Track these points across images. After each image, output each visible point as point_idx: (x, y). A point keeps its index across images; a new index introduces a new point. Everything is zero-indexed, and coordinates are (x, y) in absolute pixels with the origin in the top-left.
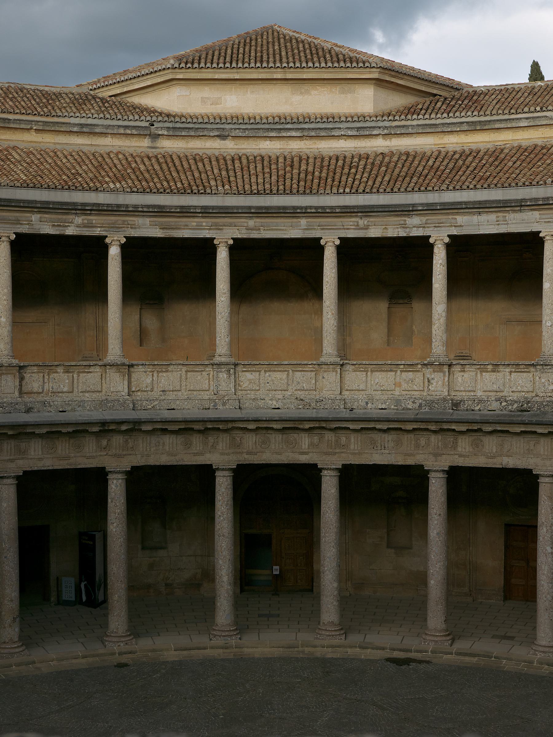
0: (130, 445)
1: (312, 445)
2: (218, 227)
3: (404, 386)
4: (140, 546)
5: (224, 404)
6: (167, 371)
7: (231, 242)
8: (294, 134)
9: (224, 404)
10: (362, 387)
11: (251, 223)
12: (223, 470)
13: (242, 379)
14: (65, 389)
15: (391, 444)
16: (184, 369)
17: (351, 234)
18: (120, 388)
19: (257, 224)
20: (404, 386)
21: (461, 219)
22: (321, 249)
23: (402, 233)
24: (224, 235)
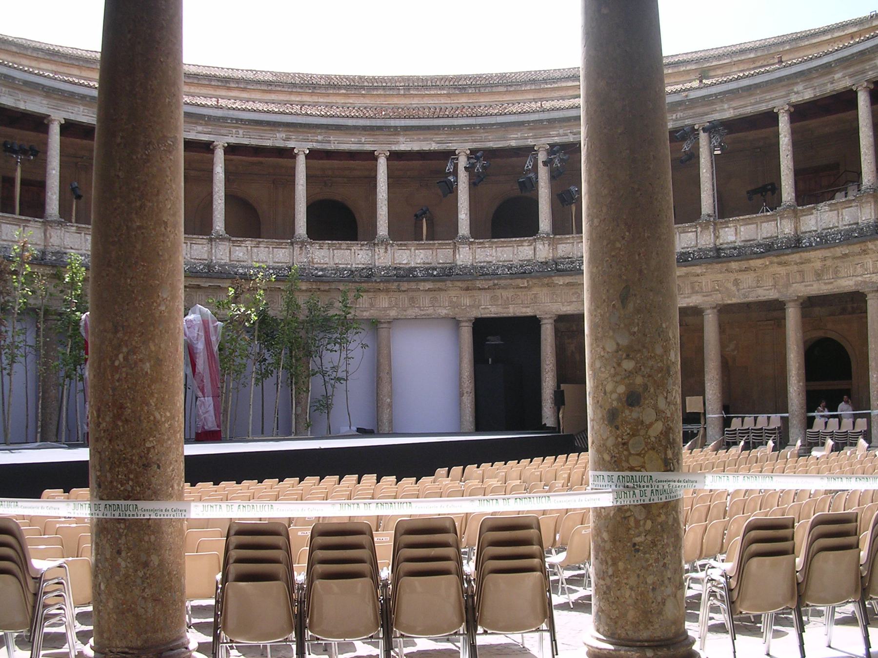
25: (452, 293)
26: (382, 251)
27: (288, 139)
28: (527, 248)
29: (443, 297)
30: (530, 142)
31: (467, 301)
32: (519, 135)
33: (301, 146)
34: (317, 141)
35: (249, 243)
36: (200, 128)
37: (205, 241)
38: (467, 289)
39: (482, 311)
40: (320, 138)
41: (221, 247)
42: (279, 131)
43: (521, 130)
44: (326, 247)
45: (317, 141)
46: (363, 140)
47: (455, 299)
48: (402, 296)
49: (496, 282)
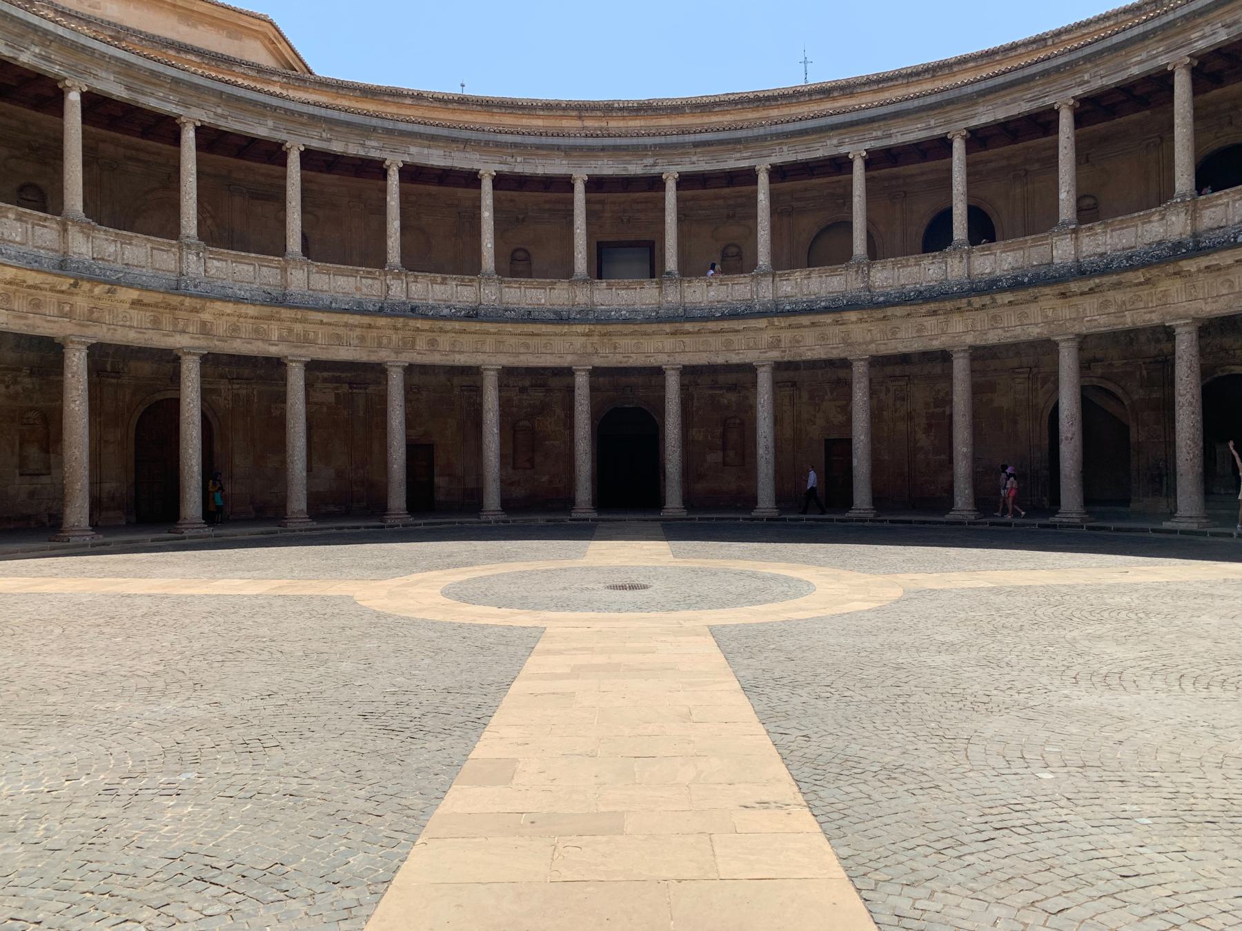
0: (95, 315)
1: (280, 336)
2: (186, 105)
3: (364, 290)
4: (17, 471)
5: (196, 286)
6: (130, 244)
7: (199, 124)
8: (193, 58)
9: (196, 286)
10: (325, 287)
11: (219, 111)
12: (194, 354)
13: (209, 265)
14: (18, 239)
15: (356, 342)
16: (149, 245)
17: (315, 144)
18: (84, 250)
19: (226, 113)
20: (364, 290)
21: (413, 150)
22: (284, 156)
23: (362, 153)
24: (192, 117)
25: (1043, 303)
26: (956, 261)
27: (841, 144)
28: (1156, 224)
29: (1034, 309)
30: (1162, 61)
31: (1067, 313)
32: (1144, 56)
33: (856, 149)
34: (876, 138)
35: (798, 275)
36: (738, 155)
37: (748, 280)
38: (1063, 295)
39: (1087, 325)
40: (879, 133)
41: (764, 284)
42: (830, 138)
43: (1147, 47)
44: (889, 265)
45: (876, 138)
46: (932, 122)
47: (1050, 313)
48: (982, 315)
49: (1097, 281)
